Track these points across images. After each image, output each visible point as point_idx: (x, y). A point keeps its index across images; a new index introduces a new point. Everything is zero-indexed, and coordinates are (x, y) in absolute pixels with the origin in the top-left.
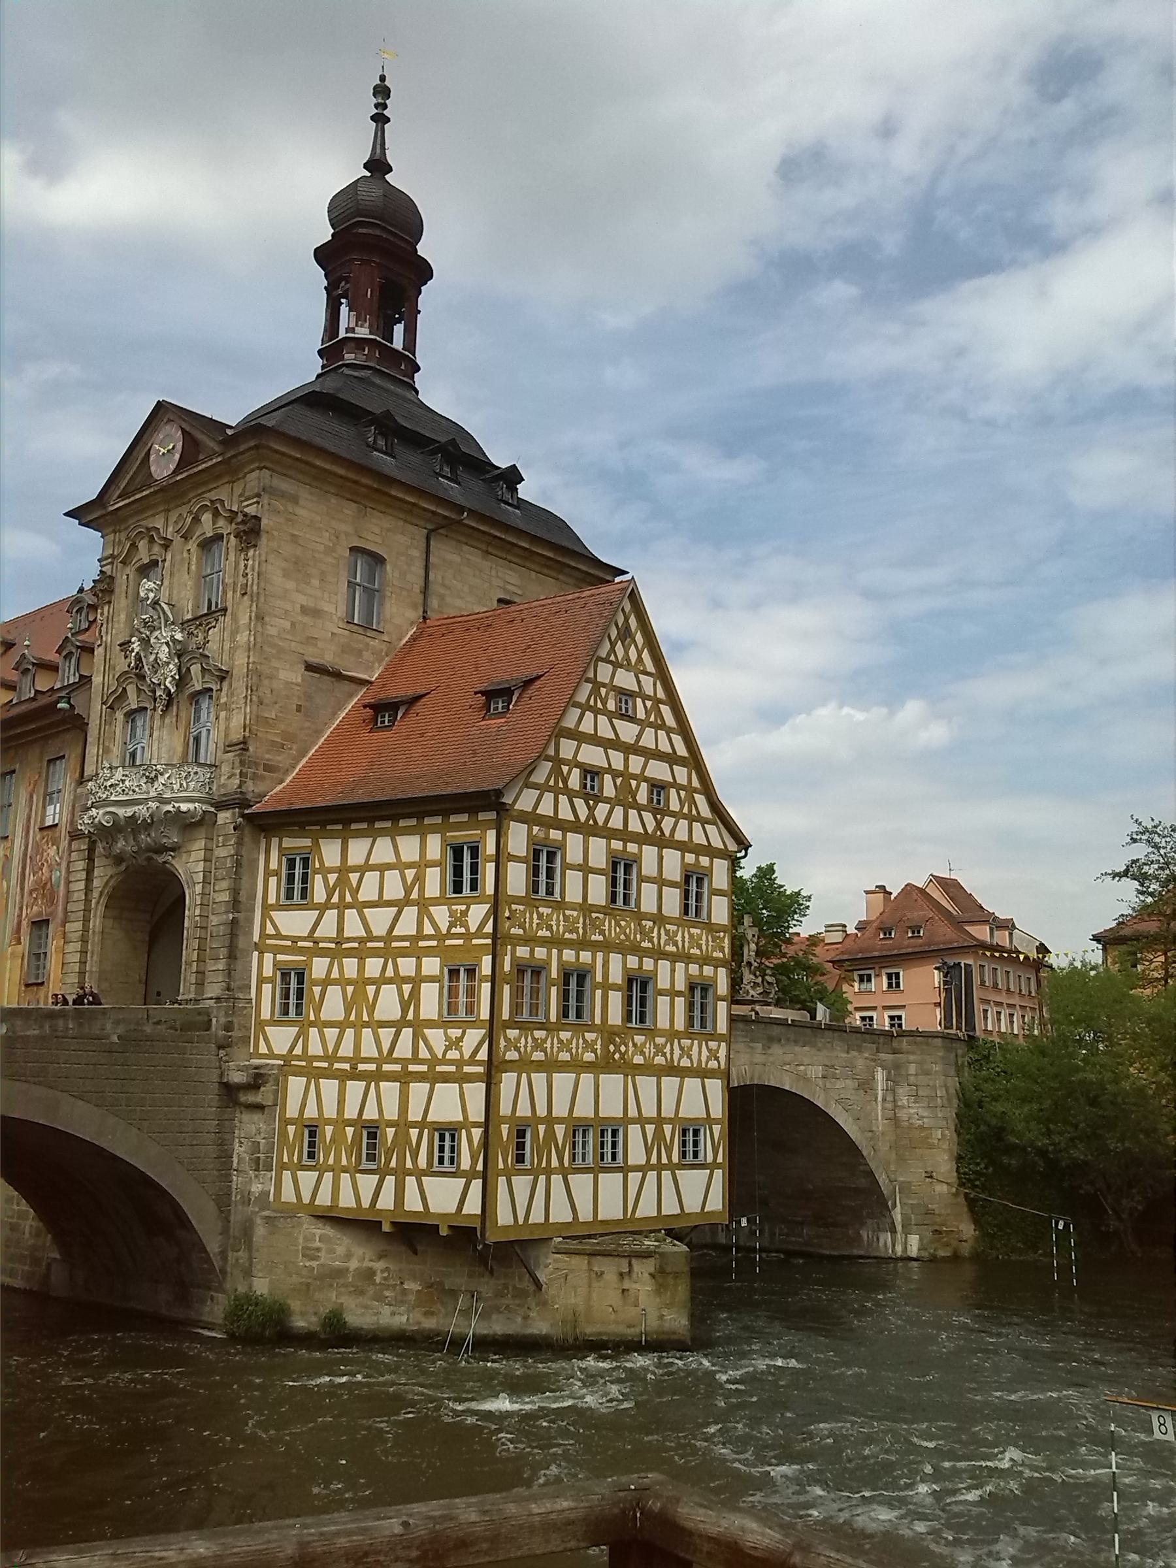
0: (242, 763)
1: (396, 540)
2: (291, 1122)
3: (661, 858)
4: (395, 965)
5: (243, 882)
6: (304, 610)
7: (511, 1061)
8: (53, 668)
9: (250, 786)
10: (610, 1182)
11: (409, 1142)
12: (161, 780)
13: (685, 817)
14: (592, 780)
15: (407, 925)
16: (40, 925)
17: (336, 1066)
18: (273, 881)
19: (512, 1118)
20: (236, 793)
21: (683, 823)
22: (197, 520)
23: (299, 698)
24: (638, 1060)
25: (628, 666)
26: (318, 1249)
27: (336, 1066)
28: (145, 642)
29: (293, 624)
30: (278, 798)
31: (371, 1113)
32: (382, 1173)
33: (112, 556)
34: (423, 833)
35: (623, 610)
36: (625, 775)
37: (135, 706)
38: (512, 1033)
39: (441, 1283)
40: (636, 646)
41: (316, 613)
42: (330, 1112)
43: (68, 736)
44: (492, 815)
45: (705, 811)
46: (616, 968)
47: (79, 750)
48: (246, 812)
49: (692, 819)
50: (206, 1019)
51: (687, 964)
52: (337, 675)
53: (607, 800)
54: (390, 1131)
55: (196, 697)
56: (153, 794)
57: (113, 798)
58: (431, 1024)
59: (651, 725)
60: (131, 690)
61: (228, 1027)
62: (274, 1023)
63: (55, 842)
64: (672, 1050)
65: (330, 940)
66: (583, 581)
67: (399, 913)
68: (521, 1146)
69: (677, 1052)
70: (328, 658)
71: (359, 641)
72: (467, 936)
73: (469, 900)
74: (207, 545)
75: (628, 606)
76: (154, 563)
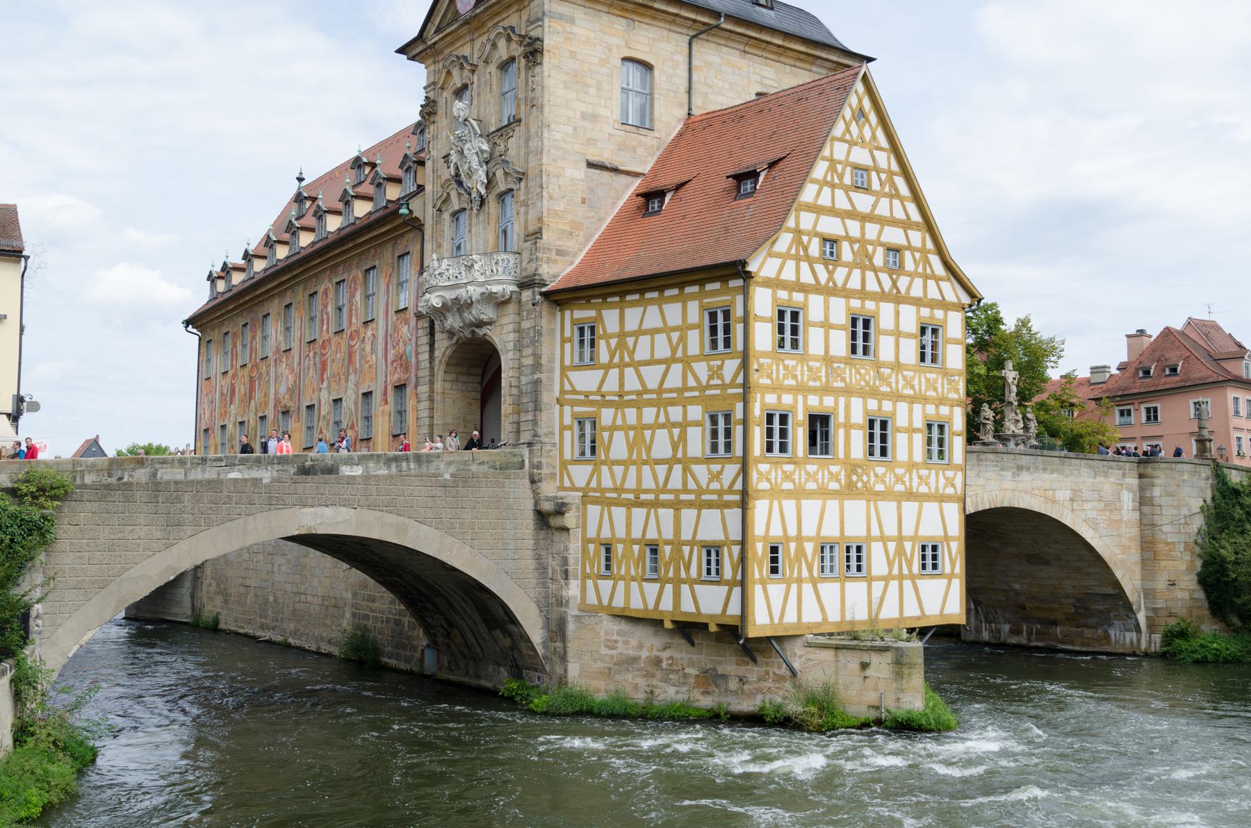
1: (662, 44)
2: (590, 541)
3: (897, 313)
4: (666, 414)
6: (584, 116)
8: (398, 181)
9: (546, 271)
10: (856, 590)
11: (682, 557)
12: (476, 267)
13: (919, 275)
14: (832, 248)
15: (674, 380)
16: (400, 388)
17: (624, 496)
19: (765, 538)
21: (918, 282)
22: (494, 46)
24: (880, 487)
25: (862, 142)
26: (616, 642)
27: (624, 496)
28: (461, 153)
29: (575, 129)
30: (569, 277)
31: (652, 534)
32: (662, 581)
33: (434, 83)
35: (856, 92)
36: (863, 241)
37: (457, 208)
38: (764, 467)
39: (715, 669)
40: (870, 125)
41: (594, 118)
42: (621, 532)
43: (411, 236)
44: (739, 282)
45: (939, 269)
46: (858, 411)
47: (419, 247)
48: (544, 290)
49: (926, 277)
51: (924, 405)
52: (615, 170)
53: (846, 265)
54: (668, 549)
55: (501, 196)
58: (697, 461)
59: (885, 195)
60: (453, 195)
61: (539, 466)
63: (406, 322)
64: (911, 479)
65: (614, 394)
66: (834, 70)
67: (667, 369)
68: (774, 560)
69: (916, 481)
70: (606, 157)
71: (634, 139)
72: (724, 387)
74: (504, 66)
75: (859, 87)
76: (465, 87)
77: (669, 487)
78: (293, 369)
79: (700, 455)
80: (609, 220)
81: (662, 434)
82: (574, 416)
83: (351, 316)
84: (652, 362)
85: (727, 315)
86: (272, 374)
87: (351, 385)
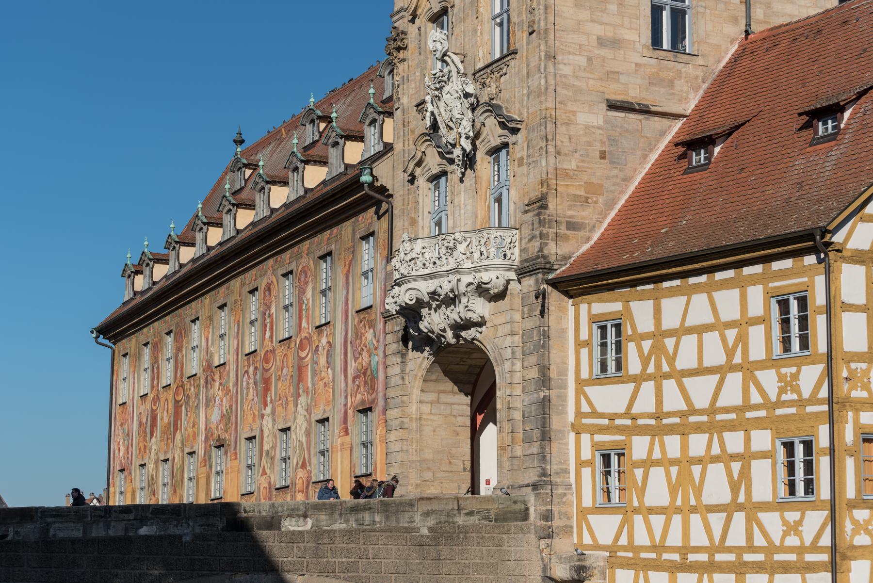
0: (542, 223)
5: (551, 355)
6: (602, 42)
7: (861, 547)
12: (461, 248)
15: (732, 392)
17: (666, 556)
18: (585, 352)
20: (538, 257)
23: (603, 143)
27: (666, 556)
29: (590, 59)
34: (742, 284)
38: (861, 515)
41: (615, 43)
48: (550, 277)
50: (523, 507)
52: (645, 111)
56: (452, 264)
57: (414, 273)
58: (766, 507)
61: (547, 516)
62: (598, 510)
63: (372, 325)
65: (650, 416)
70: (634, 94)
72: (801, 403)
73: (798, 361)
77: (728, 543)
78: (227, 392)
79: (769, 498)
80: (639, 179)
81: (716, 471)
82: (595, 446)
83: (300, 319)
84: (701, 371)
85: (803, 302)
86: (202, 398)
87: (301, 411)
